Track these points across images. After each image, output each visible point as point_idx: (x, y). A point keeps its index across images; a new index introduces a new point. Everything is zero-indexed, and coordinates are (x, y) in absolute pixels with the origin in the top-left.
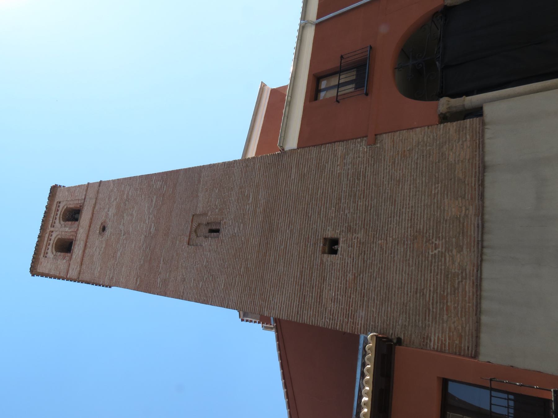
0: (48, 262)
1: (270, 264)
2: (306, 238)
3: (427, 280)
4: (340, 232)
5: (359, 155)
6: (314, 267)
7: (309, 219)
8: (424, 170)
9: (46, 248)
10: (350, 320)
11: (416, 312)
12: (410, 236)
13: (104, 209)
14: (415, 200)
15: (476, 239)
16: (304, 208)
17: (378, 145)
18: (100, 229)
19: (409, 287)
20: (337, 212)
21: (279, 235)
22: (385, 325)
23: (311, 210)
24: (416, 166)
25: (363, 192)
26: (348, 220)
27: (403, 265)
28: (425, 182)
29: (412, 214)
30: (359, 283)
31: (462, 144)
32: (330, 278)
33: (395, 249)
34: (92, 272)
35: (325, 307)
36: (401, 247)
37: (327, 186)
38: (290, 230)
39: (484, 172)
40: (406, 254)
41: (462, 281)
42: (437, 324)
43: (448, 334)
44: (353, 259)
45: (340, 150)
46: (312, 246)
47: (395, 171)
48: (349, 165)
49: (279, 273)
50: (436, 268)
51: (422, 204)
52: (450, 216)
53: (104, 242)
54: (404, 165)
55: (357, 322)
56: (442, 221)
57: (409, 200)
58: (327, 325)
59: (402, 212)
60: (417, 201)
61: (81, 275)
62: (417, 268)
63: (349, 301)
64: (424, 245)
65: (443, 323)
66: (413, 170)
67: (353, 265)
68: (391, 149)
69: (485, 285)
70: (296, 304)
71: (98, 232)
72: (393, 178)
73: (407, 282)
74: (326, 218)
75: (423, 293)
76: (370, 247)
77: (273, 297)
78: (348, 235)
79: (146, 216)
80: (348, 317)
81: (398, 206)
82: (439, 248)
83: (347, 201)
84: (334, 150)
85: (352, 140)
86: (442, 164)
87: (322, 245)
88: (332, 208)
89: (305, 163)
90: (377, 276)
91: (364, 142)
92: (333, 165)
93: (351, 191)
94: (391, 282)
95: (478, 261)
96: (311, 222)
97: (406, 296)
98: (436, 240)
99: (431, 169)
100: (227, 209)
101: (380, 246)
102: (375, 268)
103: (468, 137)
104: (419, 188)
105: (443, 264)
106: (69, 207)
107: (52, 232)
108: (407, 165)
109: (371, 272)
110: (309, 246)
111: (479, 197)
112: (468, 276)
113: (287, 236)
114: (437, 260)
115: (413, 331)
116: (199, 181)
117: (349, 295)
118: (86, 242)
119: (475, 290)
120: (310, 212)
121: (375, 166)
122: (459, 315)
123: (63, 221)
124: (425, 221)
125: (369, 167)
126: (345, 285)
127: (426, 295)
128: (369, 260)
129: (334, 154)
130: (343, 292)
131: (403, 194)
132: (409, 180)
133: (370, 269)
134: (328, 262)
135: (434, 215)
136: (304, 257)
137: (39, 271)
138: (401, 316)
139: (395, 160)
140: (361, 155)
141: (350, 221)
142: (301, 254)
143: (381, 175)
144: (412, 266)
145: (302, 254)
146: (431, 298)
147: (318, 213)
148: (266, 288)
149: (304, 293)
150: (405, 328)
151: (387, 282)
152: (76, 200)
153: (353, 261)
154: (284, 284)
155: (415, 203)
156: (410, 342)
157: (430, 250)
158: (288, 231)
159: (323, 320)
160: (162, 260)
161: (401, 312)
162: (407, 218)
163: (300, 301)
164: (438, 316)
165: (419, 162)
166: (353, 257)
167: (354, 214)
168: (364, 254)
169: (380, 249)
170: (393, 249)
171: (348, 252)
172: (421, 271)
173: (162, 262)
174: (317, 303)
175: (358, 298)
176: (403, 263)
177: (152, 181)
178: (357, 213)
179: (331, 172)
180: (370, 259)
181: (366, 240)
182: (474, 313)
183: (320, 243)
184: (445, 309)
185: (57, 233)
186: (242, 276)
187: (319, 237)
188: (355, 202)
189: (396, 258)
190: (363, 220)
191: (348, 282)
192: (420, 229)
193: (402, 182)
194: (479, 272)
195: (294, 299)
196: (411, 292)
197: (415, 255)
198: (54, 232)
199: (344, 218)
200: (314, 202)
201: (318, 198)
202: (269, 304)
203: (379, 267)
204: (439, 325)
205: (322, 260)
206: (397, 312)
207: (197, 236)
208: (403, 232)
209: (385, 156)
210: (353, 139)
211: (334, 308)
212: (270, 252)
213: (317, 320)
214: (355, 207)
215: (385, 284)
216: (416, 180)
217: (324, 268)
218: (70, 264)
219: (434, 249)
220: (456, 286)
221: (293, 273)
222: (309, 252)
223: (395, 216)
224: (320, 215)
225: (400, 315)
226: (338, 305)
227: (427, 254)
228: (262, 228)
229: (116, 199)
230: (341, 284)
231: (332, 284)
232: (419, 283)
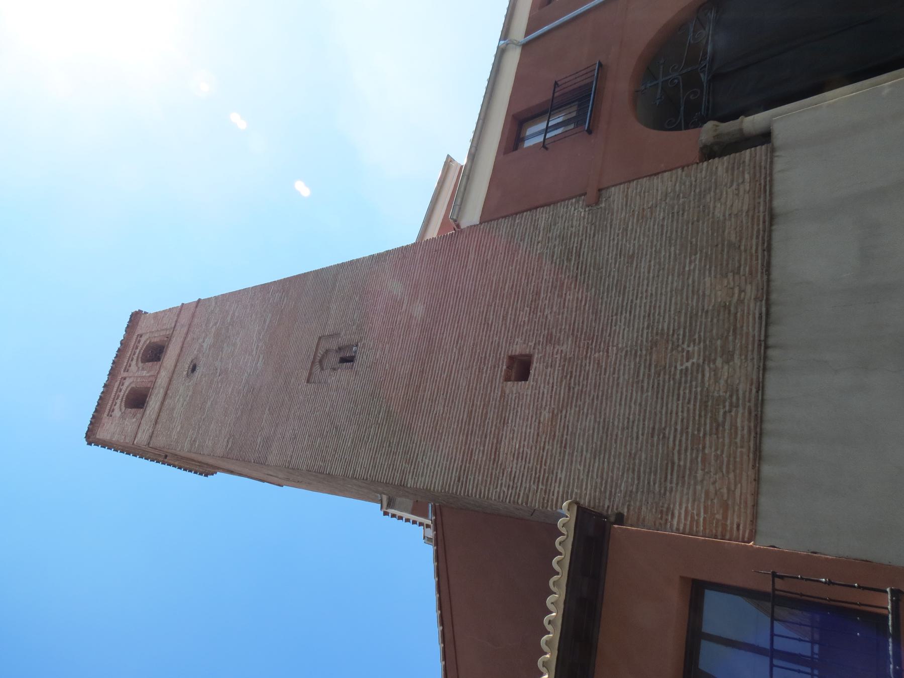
0: (112, 423)
2: (481, 358)
3: (671, 413)
4: (535, 344)
5: (572, 223)
6: (491, 403)
7: (489, 328)
8: (674, 236)
9: (113, 403)
10: (540, 486)
11: (650, 469)
12: (646, 341)
13: (198, 339)
14: (657, 284)
15: (757, 338)
16: (483, 312)
17: (603, 205)
18: (189, 369)
19: (641, 426)
20: (532, 314)
21: (441, 357)
22: (597, 494)
23: (493, 315)
24: (660, 230)
25: (574, 279)
26: (549, 326)
27: (632, 390)
28: (675, 254)
29: (650, 307)
30: (560, 425)
31: (738, 189)
32: (514, 420)
33: (620, 365)
35: (503, 467)
36: (630, 361)
37: (520, 275)
38: (458, 347)
39: (771, 224)
40: (638, 372)
41: (730, 411)
42: (686, 486)
43: (704, 502)
44: (553, 387)
45: (544, 219)
46: (490, 370)
47: (626, 241)
48: (556, 239)
49: (435, 417)
50: (687, 391)
51: (669, 289)
52: (713, 304)
53: (191, 388)
54: (642, 232)
55: (552, 490)
56: (700, 314)
57: (648, 285)
58: (503, 498)
59: (636, 304)
60: (659, 285)
61: (153, 439)
62: (655, 394)
63: (541, 455)
64: (669, 355)
65: (695, 484)
66: (655, 237)
67: (551, 396)
68: (622, 209)
69: (770, 411)
70: (458, 464)
71: (185, 373)
72: (623, 252)
73: (637, 416)
74: (515, 324)
75: (664, 434)
76: (581, 366)
77: (423, 455)
78: (548, 348)
80: (539, 481)
81: (628, 295)
82: (694, 357)
83: (549, 294)
84: (535, 220)
85: (563, 203)
86: (703, 223)
87: (505, 367)
88: (526, 308)
89: (490, 243)
90: (590, 411)
91: (581, 202)
92: (531, 242)
94: (611, 421)
95: (759, 374)
96: (492, 332)
97: (634, 442)
98: (689, 346)
99: (684, 232)
101: (597, 362)
102: (587, 400)
103: (747, 176)
104: (664, 265)
105: (699, 385)
106: (153, 341)
108: (647, 230)
109: (580, 406)
111: (762, 270)
112: (741, 402)
113: (453, 357)
114: (689, 378)
115: (644, 500)
117: (542, 445)
118: (168, 389)
119: (752, 425)
120: (491, 317)
121: (596, 238)
122: (724, 470)
123: (142, 362)
124: (672, 316)
125: (586, 240)
126: (536, 429)
127: (669, 438)
128: (577, 386)
129: (534, 225)
130: (533, 442)
131: (638, 275)
132: (649, 253)
133: (579, 400)
134: (512, 394)
135: (688, 304)
136: (476, 389)
137: (98, 437)
138: (625, 475)
139: (628, 225)
140: (574, 224)
141: (551, 327)
142: (471, 385)
143: (604, 251)
144: (647, 391)
145: (473, 384)
146: (677, 443)
147: (503, 317)
149: (471, 447)
150: (630, 496)
151: (604, 419)
152: (163, 330)
153: (552, 390)
155: (657, 288)
156: (638, 519)
157: (679, 363)
159: (498, 490)
160: (267, 409)
161: (626, 470)
162: (642, 313)
163: (465, 460)
164: (687, 472)
165: (665, 223)
166: (553, 383)
167: (559, 315)
168: (571, 377)
169: (596, 366)
170: (617, 365)
171: (546, 375)
172: (662, 399)
173: (267, 411)
174: (490, 461)
175: (556, 449)
176: (632, 386)
177: (269, 293)
178: (563, 313)
179: (527, 252)
180: (579, 385)
181: (574, 355)
182: (751, 466)
183: (502, 364)
184: (699, 459)
185: (131, 380)
186: (379, 424)
187: (502, 355)
188: (562, 296)
190: (572, 322)
191: (541, 425)
192: (663, 329)
193: (637, 257)
194: (760, 392)
195: (456, 456)
196: (643, 435)
197: (653, 370)
198: (127, 379)
199: (542, 323)
200: (498, 301)
201: (505, 294)
202: (416, 467)
203: (594, 396)
204: (688, 488)
205: (503, 392)
206: (618, 469)
207: (322, 369)
208: (635, 336)
209: (612, 220)
210: (564, 200)
211: (516, 468)
212: (425, 384)
213: (489, 490)
214: (560, 303)
215: (601, 424)
216: (660, 252)
217: (505, 403)
219: (685, 360)
220: (721, 419)
221: (458, 415)
222: (485, 380)
223: (624, 312)
224: (507, 319)
225: (623, 475)
226: (524, 463)
227: (673, 369)
228: (417, 349)
229: (216, 324)
230: (530, 428)
232: (658, 418)
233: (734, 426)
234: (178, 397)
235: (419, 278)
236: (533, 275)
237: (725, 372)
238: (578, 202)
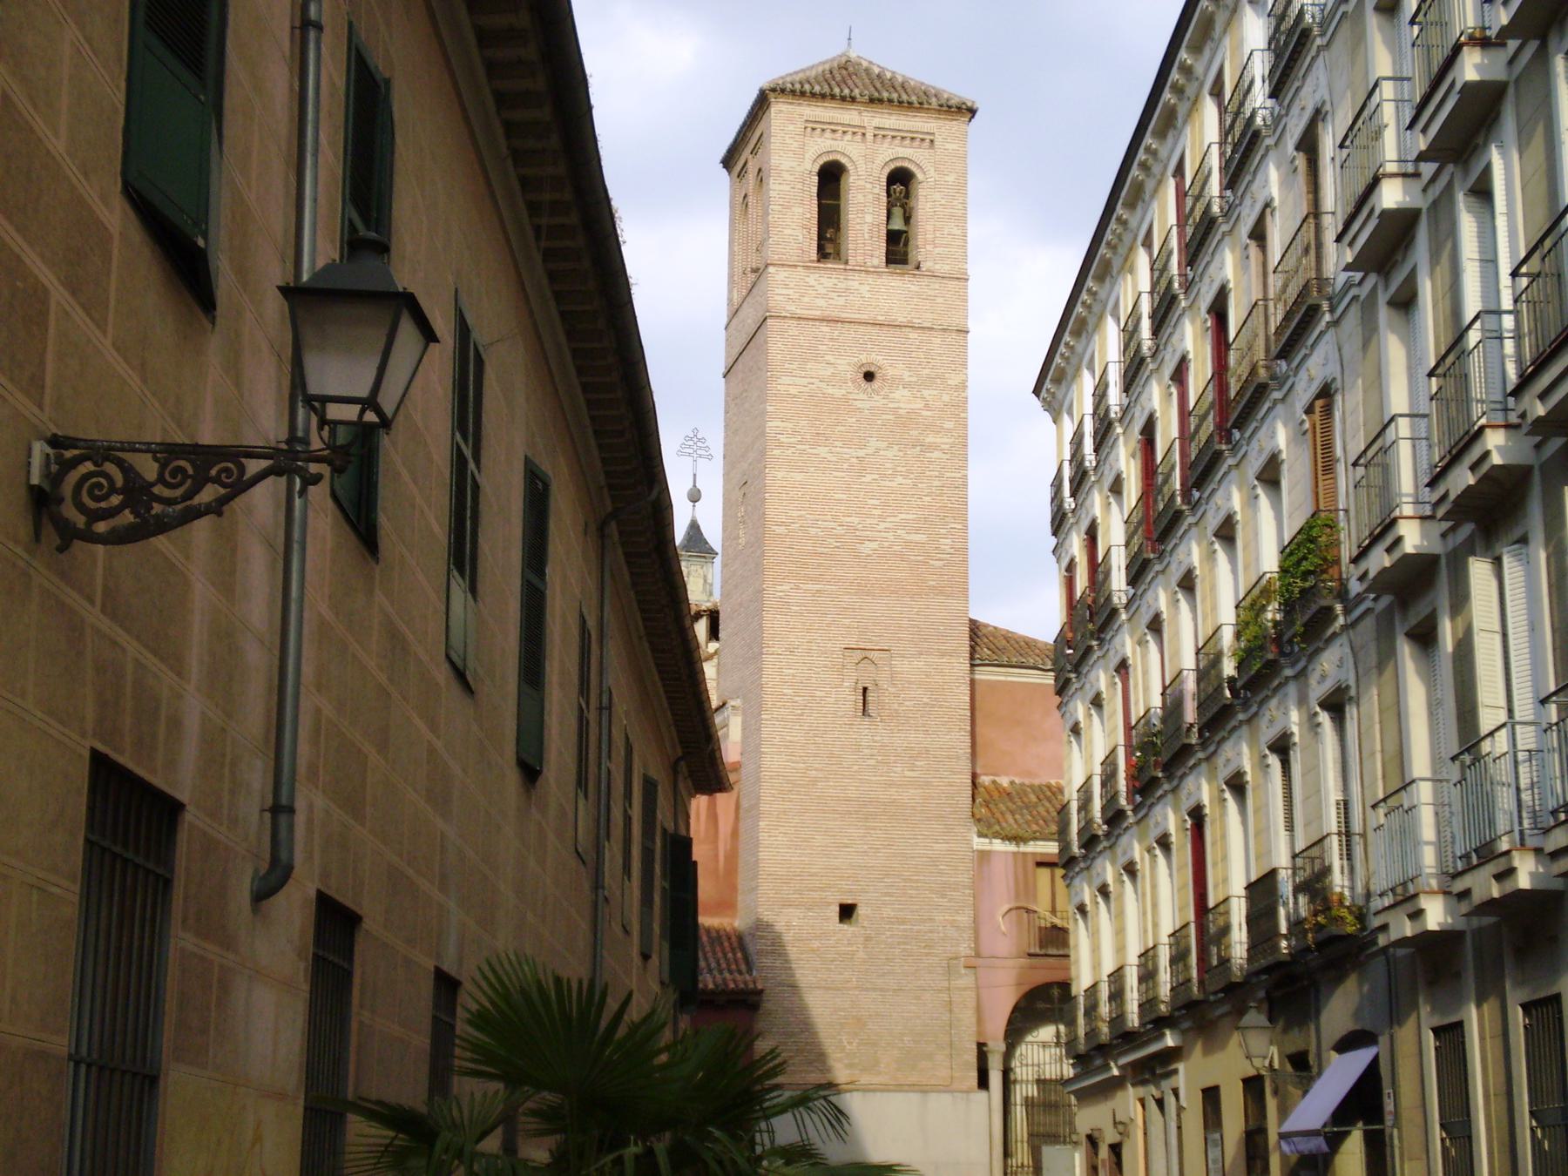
34: (787, 366)
71: (864, 358)
116: (943, 654)
205: (829, 904)
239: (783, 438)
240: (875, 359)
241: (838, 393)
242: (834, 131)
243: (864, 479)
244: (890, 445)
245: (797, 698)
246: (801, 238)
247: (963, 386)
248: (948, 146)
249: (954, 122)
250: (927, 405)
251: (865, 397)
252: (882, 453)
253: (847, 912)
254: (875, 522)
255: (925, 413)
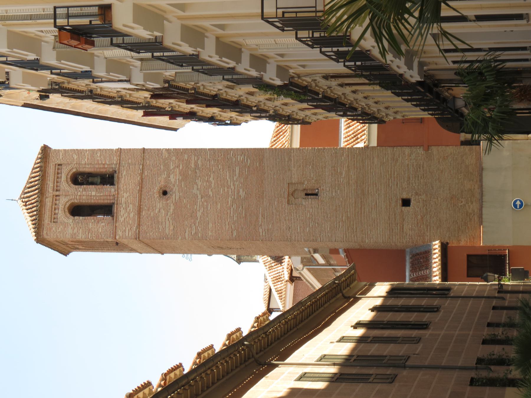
1: (366, 214)
17: (430, 151)
31: (472, 157)
34: (161, 230)
39: (482, 171)
69: (484, 216)
71: (156, 196)
79: (229, 182)
88: (405, 183)
93: (416, 174)
100: (323, 181)
103: (474, 154)
107: (56, 196)
110: (392, 203)
116: (290, 160)
135: (460, 188)
136: (389, 209)
140: (420, 155)
148: (364, 227)
154: (378, 224)
158: (376, 195)
173: (260, 216)
189: (443, 207)
205: (402, 211)
218: (116, 226)
224: (398, 186)
231: (409, 222)
233: (474, 219)
234: (158, 210)
235: (349, 164)
236: (406, 171)
237: (471, 207)
238: (420, 148)
239: (193, 232)
240: (156, 190)
241: (172, 207)
242: (55, 209)
243: (211, 195)
244: (196, 183)
245: (311, 225)
246: (103, 224)
247: (168, 150)
248: (61, 157)
249: (50, 155)
250: (178, 167)
251: (174, 195)
252: (199, 187)
253: (406, 203)
254: (230, 190)
255: (181, 168)
